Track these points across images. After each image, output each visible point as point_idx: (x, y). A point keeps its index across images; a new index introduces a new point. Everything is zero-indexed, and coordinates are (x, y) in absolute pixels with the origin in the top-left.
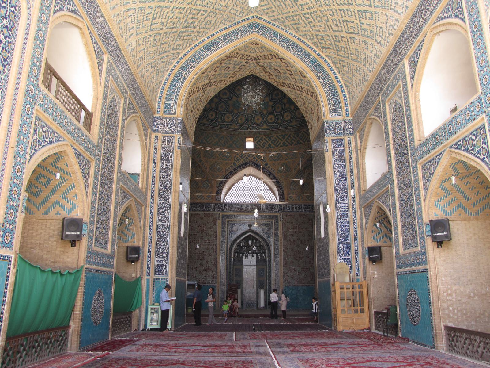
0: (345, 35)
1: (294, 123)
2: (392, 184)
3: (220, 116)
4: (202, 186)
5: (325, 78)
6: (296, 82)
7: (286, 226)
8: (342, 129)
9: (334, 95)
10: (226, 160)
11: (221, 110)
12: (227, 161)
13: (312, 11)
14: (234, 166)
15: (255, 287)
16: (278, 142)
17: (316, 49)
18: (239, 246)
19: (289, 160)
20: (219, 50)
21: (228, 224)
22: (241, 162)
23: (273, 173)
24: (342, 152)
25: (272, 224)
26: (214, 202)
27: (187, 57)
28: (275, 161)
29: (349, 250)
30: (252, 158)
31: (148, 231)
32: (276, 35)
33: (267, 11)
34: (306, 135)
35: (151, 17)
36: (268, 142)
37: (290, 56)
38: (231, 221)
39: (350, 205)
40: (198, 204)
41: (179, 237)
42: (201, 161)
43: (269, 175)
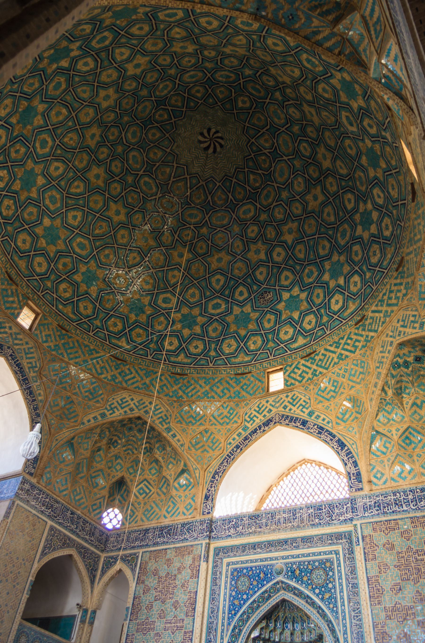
1: (352, 307)
3: (213, 346)
4: (177, 485)
7: (375, 558)
10: (228, 424)
11: (214, 335)
12: (228, 427)
14: (243, 433)
16: (328, 360)
19: (358, 387)
21: (227, 571)
22: (257, 421)
23: (328, 427)
25: (338, 559)
26: (199, 518)
28: (328, 400)
30: (281, 409)
34: (377, 315)
36: (310, 368)
38: (233, 563)
40: (166, 527)
42: (169, 430)
43: (320, 433)
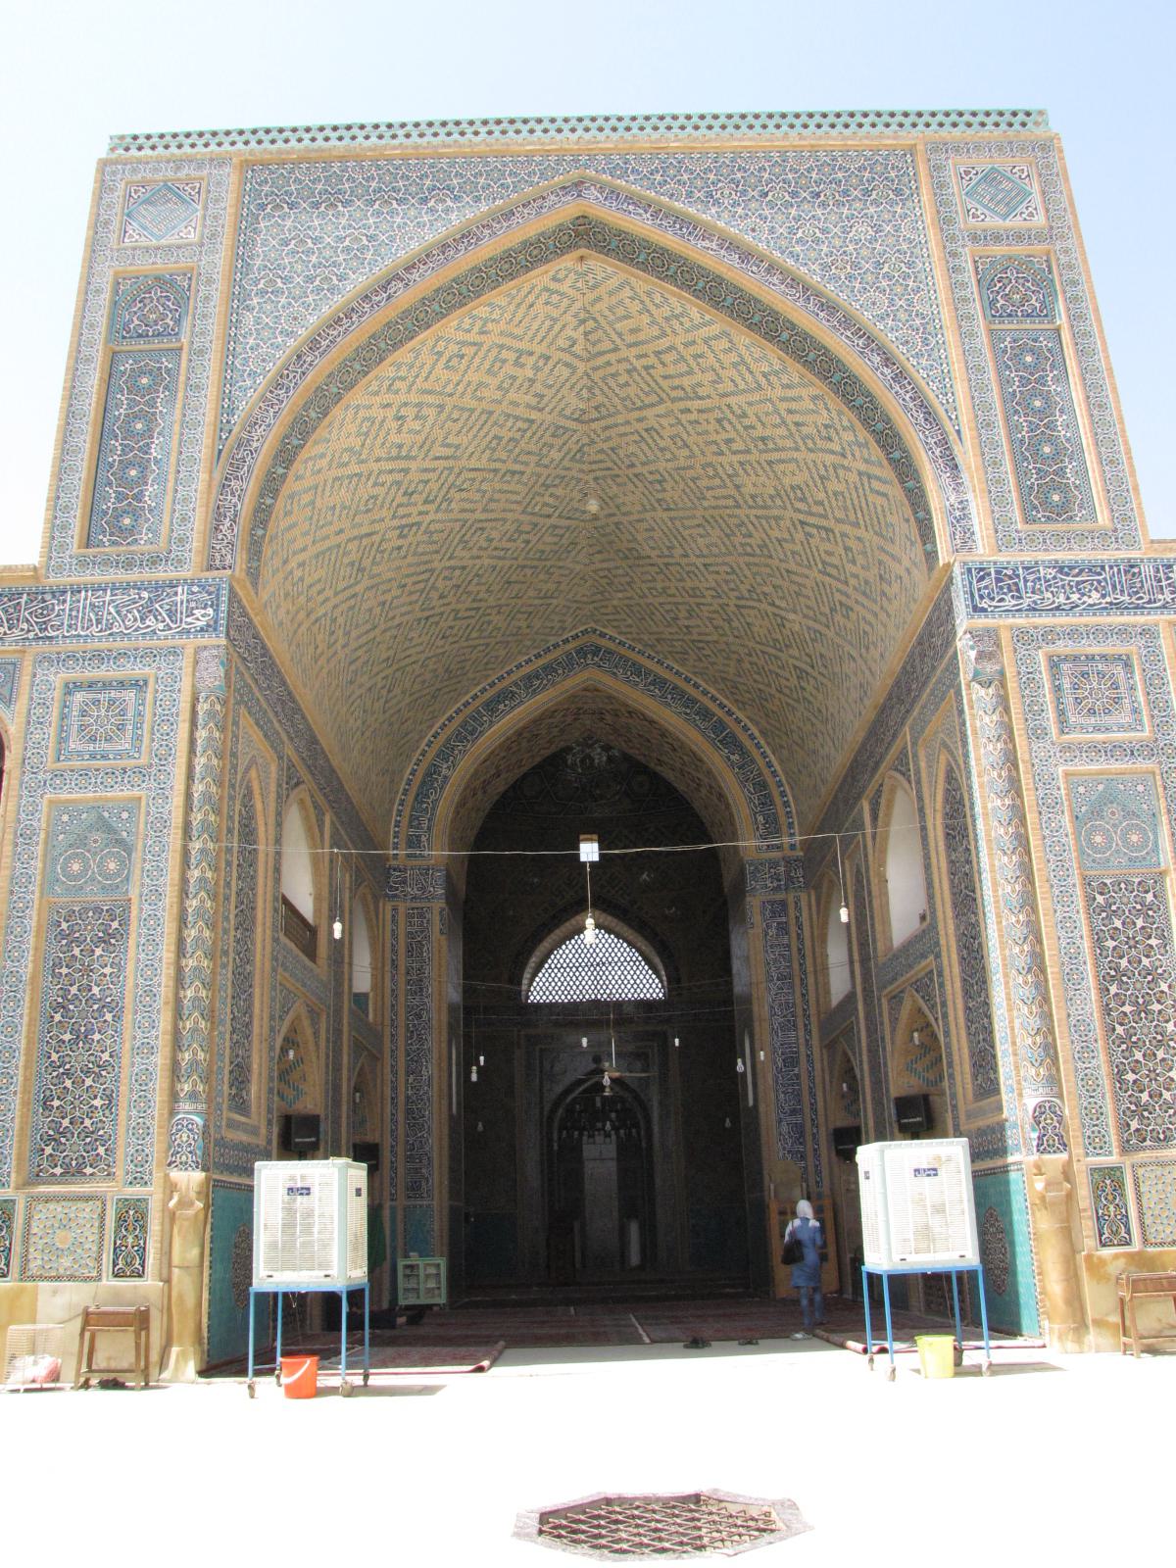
0: (778, 695)
2: (857, 1018)
5: (744, 764)
6: (684, 764)
8: (783, 877)
9: (766, 802)
13: (709, 638)
15: (615, 1214)
17: (725, 702)
18: (570, 1110)
20: (516, 712)
24: (783, 929)
27: (448, 731)
29: (802, 1134)
31: (388, 1109)
32: (638, 670)
33: (615, 624)
35: (384, 692)
37: (670, 717)
39: (802, 1041)
41: (451, 1116)
